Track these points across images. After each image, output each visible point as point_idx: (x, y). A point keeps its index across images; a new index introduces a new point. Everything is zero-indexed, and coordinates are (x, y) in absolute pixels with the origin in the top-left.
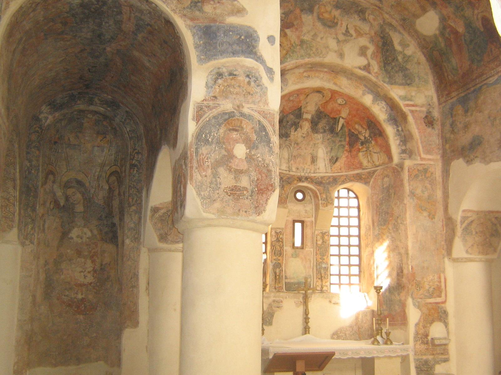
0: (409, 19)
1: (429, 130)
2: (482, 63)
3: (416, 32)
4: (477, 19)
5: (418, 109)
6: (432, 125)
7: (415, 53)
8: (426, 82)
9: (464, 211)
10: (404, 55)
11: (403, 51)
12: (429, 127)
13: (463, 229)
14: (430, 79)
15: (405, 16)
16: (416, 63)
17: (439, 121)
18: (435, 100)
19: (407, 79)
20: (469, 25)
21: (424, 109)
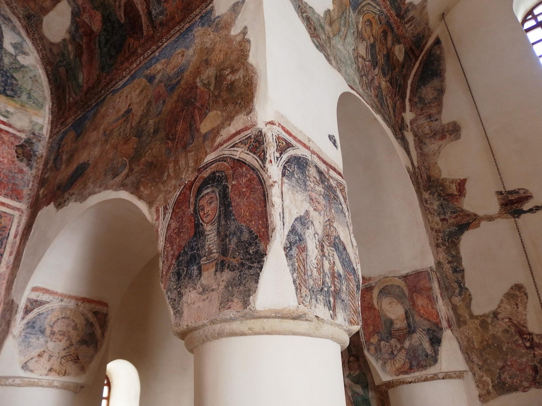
0: (34, 16)
1: (23, 165)
2: (114, 67)
3: (42, 38)
4: (120, 7)
5: (10, 130)
6: (29, 160)
7: (34, 66)
8: (41, 106)
9: (35, 289)
10: (15, 60)
11: (16, 56)
12: (21, 161)
13: (28, 323)
14: (48, 105)
15: (30, 11)
16: (30, 78)
17: (43, 158)
18: (46, 131)
19: (7, 88)
20: (107, 19)
21: (23, 136)
